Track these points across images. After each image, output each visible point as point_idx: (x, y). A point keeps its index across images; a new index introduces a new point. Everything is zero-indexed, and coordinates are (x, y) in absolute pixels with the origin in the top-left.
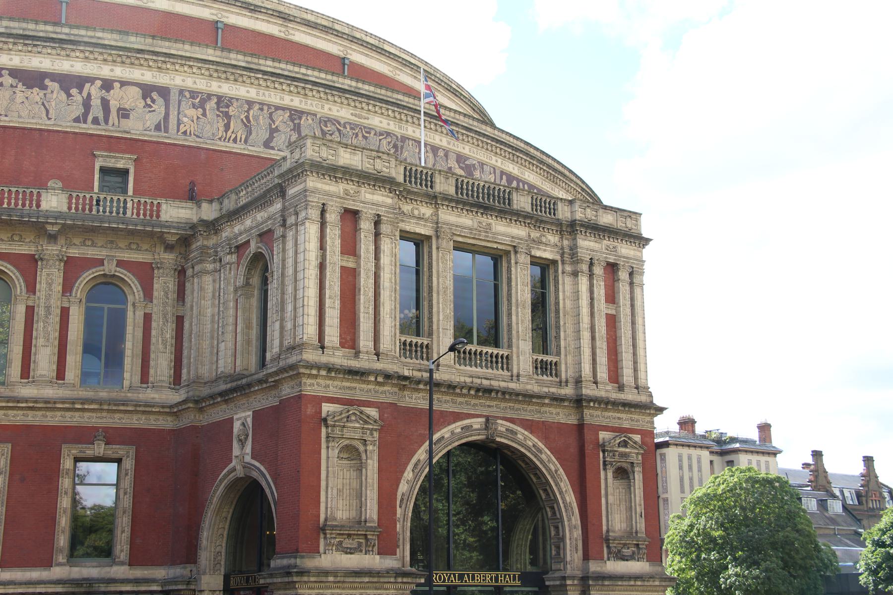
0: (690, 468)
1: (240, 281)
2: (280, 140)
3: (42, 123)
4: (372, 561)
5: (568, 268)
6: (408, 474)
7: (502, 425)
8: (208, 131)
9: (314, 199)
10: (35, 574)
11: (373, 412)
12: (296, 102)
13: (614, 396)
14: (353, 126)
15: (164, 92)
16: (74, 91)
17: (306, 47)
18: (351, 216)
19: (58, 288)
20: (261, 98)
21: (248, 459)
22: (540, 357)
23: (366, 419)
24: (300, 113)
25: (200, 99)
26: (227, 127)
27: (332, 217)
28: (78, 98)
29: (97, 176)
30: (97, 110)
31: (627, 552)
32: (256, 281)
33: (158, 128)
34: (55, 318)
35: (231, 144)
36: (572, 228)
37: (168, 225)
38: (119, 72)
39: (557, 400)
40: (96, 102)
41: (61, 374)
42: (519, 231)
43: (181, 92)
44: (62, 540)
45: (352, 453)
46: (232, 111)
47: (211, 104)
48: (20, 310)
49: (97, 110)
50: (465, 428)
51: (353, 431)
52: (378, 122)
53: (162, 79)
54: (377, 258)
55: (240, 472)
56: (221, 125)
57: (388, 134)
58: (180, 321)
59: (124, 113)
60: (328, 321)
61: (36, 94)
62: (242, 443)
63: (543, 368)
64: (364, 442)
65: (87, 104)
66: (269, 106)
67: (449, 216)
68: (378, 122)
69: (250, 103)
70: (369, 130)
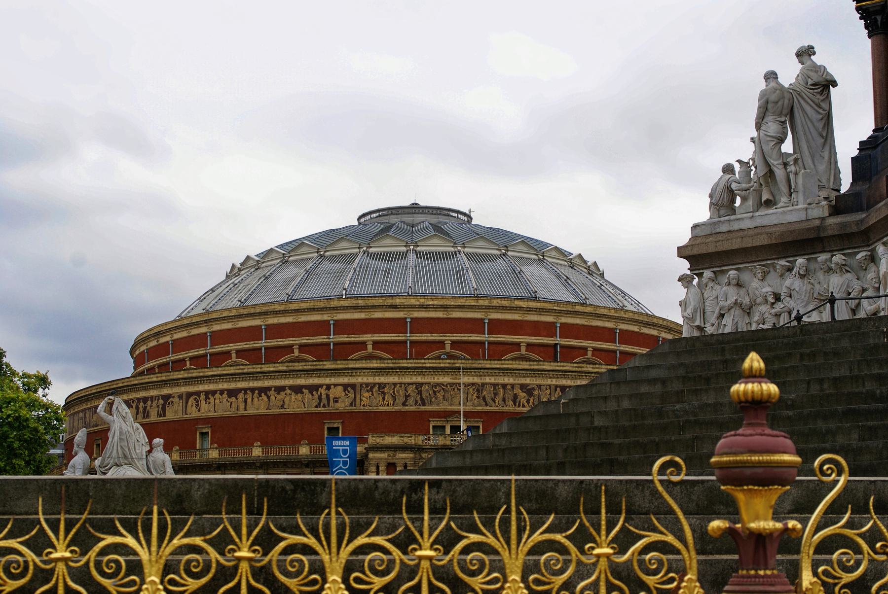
2: (411, 401)
3: (303, 410)
8: (375, 402)
12: (419, 379)
14: (451, 384)
15: (353, 386)
16: (314, 393)
17: (460, 319)
20: (400, 381)
24: (422, 384)
25: (370, 387)
26: (384, 399)
28: (316, 396)
29: (326, 432)
30: (324, 401)
33: (351, 405)
35: (386, 407)
38: (333, 380)
40: (324, 396)
43: (361, 385)
46: (386, 390)
49: (324, 401)
53: (353, 380)
56: (381, 399)
57: (473, 384)
59: (336, 400)
61: (299, 397)
65: (320, 398)
66: (405, 384)
69: (395, 384)
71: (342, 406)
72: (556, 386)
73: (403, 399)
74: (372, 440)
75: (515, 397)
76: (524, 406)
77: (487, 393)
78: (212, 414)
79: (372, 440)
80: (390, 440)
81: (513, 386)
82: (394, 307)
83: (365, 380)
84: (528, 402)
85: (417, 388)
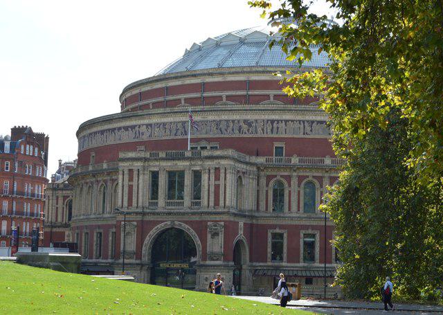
2: (179, 132)
6: (147, 238)
7: (177, 223)
9: (120, 169)
11: (135, 223)
15: (151, 125)
18: (131, 171)
25: (158, 125)
27: (125, 172)
30: (138, 135)
39: (193, 214)
47: (162, 126)
52: (211, 117)
60: (124, 200)
67: (164, 164)
68: (211, 117)
69: (171, 123)
71: (145, 138)
74: (122, 155)
76: (245, 133)
77: (223, 126)
78: (96, 146)
79: (122, 155)
80: (131, 155)
82: (195, 76)
84: (248, 130)
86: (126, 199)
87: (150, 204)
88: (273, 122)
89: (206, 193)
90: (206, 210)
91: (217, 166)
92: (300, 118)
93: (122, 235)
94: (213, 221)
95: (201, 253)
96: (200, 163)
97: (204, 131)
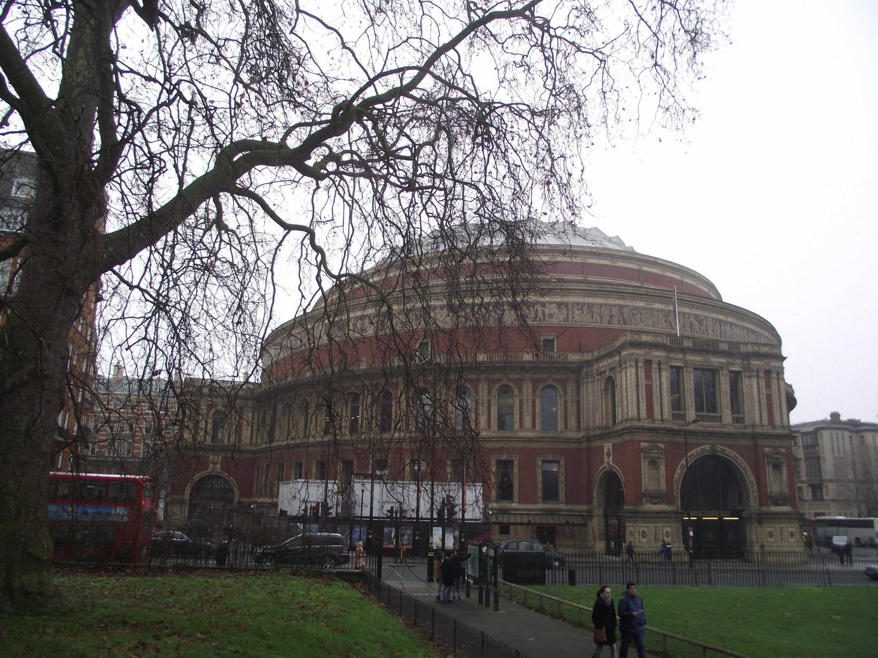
0: (838, 441)
1: (603, 388)
2: (615, 320)
4: (665, 507)
5: (747, 374)
6: (678, 471)
7: (719, 448)
10: (531, 506)
11: (662, 446)
12: (621, 302)
13: (771, 431)
14: (646, 309)
15: (566, 305)
18: (648, 363)
19: (530, 391)
21: (611, 463)
22: (735, 416)
23: (659, 449)
25: (580, 306)
26: (592, 317)
27: (640, 364)
31: (779, 502)
32: (609, 387)
33: (565, 320)
34: (530, 404)
36: (747, 356)
37: (571, 363)
39: (744, 435)
41: (534, 426)
42: (723, 360)
43: (573, 304)
44: (540, 494)
45: (654, 463)
48: (517, 401)
50: (704, 449)
51: (654, 454)
53: (565, 299)
54: (660, 379)
55: (608, 469)
57: (662, 310)
58: (578, 402)
59: (551, 316)
60: (641, 408)
62: (608, 456)
63: (736, 420)
64: (659, 458)
67: (690, 357)
69: (601, 305)
70: (653, 309)
72: (717, 320)
73: (608, 318)
75: (691, 325)
81: (689, 314)
83: (576, 300)
85: (619, 310)
86: (643, 406)
87: (675, 416)
88: (721, 322)
89: (757, 404)
90: (759, 430)
91: (768, 368)
92: (739, 323)
93: (645, 465)
94: (772, 447)
95: (756, 494)
96: (738, 361)
97: (650, 323)
